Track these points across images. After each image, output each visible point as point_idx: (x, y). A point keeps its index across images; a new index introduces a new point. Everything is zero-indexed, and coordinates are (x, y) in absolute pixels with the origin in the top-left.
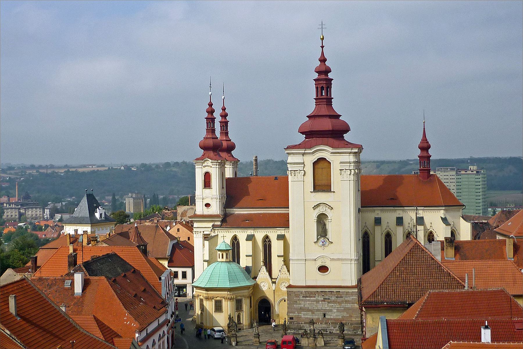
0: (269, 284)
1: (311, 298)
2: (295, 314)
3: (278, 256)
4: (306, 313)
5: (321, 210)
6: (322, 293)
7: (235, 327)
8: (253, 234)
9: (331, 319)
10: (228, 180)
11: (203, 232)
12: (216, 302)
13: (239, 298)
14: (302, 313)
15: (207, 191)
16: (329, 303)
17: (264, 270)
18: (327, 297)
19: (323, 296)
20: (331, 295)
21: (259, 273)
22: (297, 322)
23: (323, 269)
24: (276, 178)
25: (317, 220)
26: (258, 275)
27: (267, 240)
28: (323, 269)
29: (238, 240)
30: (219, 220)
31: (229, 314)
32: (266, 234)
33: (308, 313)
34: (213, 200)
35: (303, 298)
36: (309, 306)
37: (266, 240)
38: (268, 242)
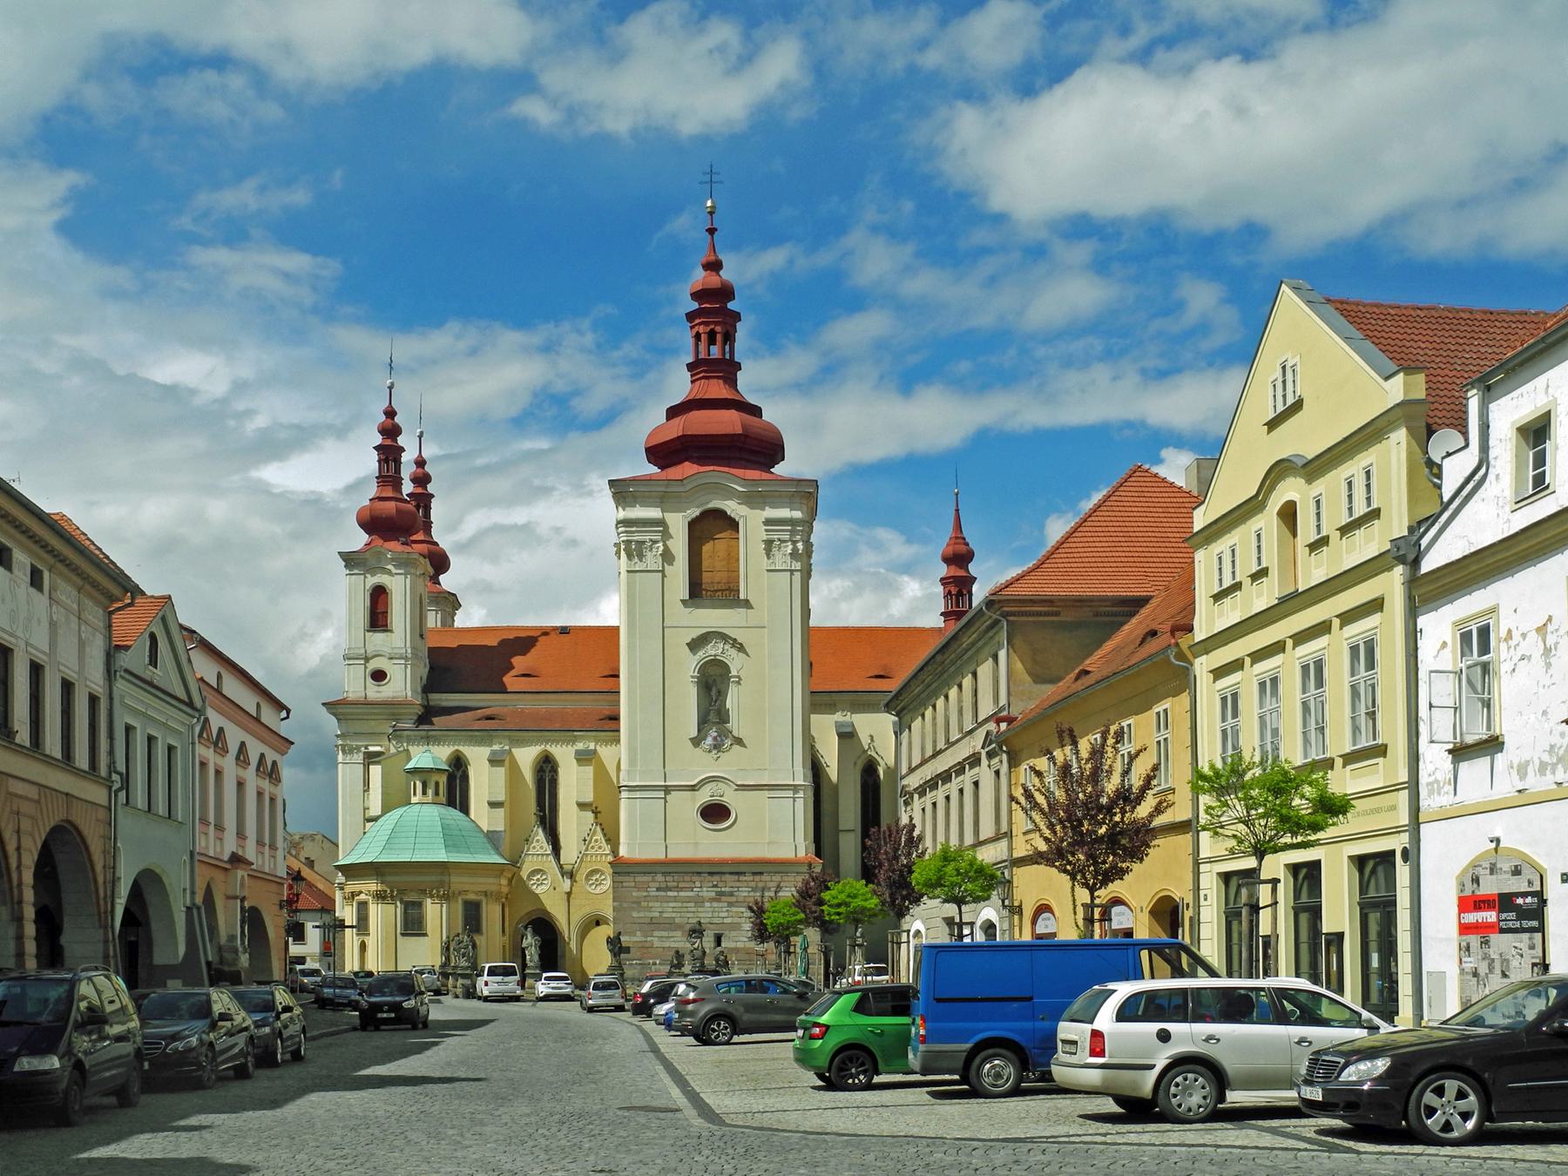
1: (682, 894)
2: (635, 939)
4: (665, 934)
5: (712, 650)
6: (710, 878)
9: (737, 950)
11: (366, 748)
13: (472, 897)
14: (656, 933)
15: (378, 638)
16: (730, 904)
18: (727, 889)
19: (716, 886)
20: (738, 884)
23: (715, 813)
25: (698, 677)
28: (715, 813)
30: (411, 714)
33: (674, 934)
35: (657, 893)
36: (674, 915)
38: (550, 772)
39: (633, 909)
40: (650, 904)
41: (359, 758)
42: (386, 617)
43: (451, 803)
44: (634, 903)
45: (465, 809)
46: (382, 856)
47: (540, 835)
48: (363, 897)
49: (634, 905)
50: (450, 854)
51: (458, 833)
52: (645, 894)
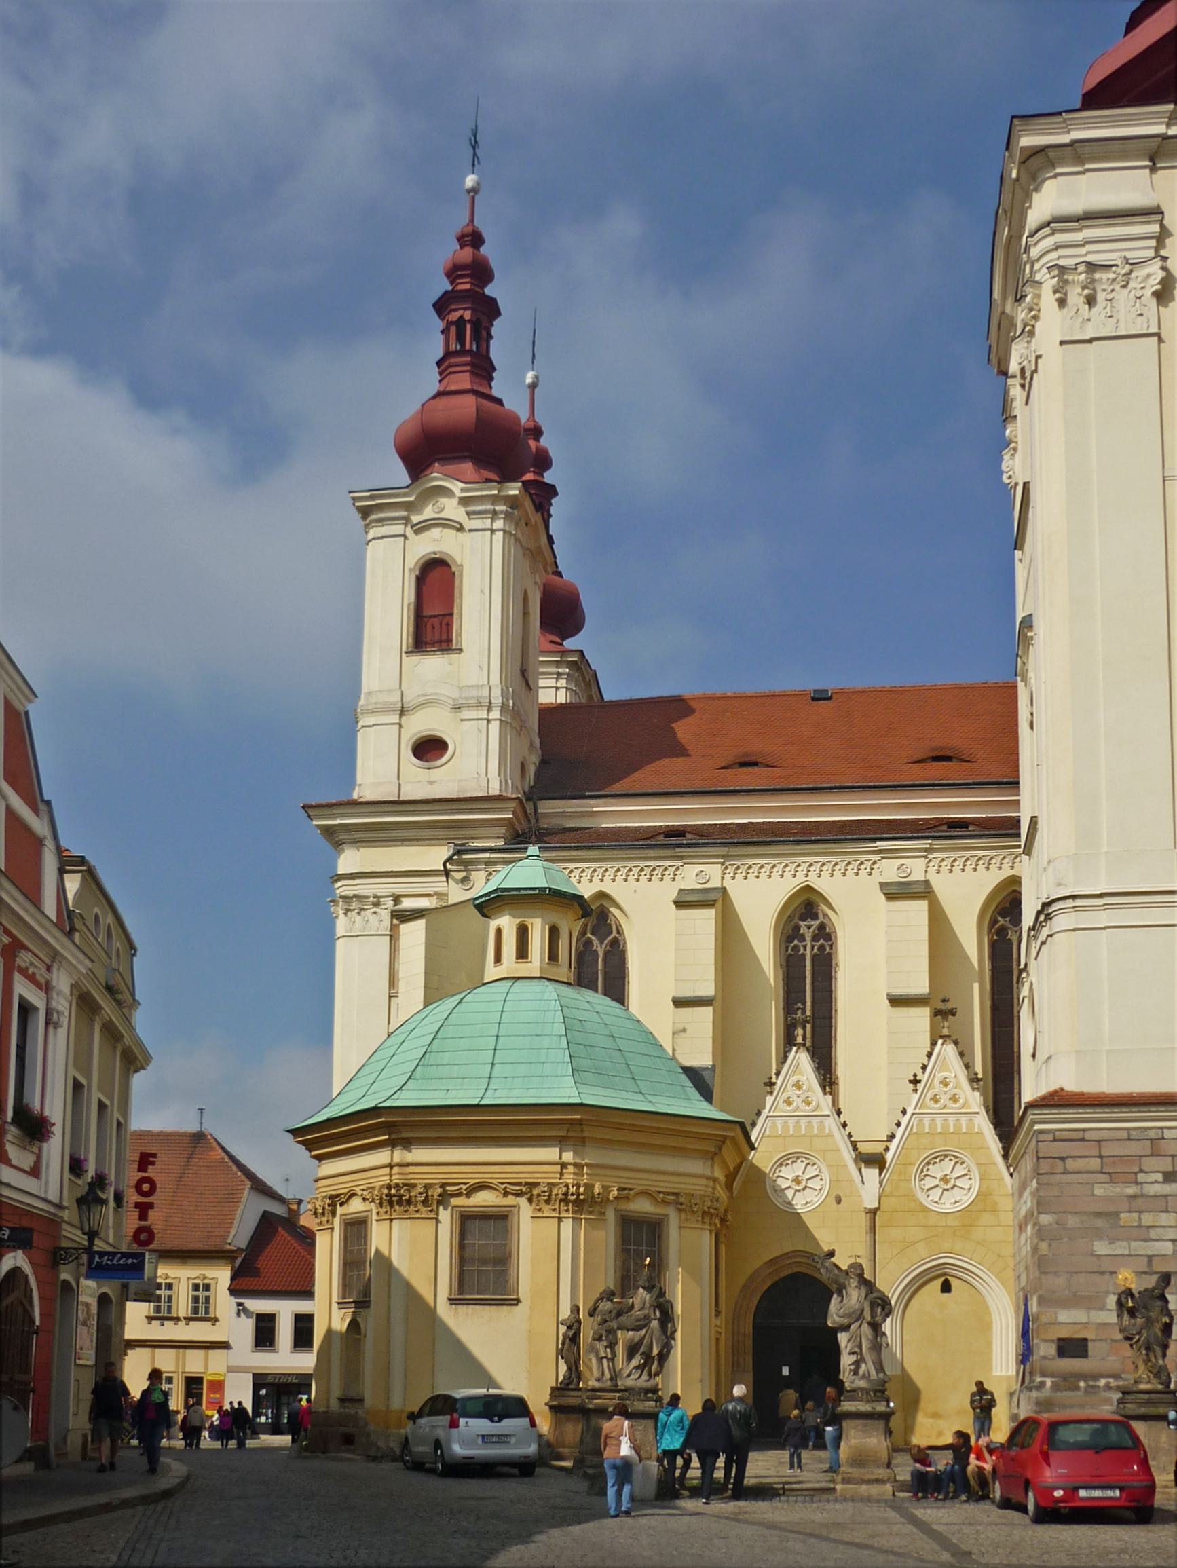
0: (837, 1168)
3: (897, 1001)
7: (655, 1324)
8: (715, 883)
10: (549, 714)
12: (466, 1220)
13: (642, 1206)
15: (432, 664)
17: (803, 1078)
21: (769, 1100)
22: (1116, 1376)
24: (820, 696)
26: (759, 1113)
27: (809, 927)
29: (614, 934)
31: (565, 1313)
32: (800, 880)
34: (466, 714)
37: (797, 928)
38: (815, 938)
39: (1098, 1234)
40: (1147, 1219)
41: (383, 918)
42: (449, 626)
43: (583, 979)
44: (1099, 1214)
45: (616, 989)
46: (403, 1094)
47: (801, 1060)
48: (356, 1206)
49: (1100, 1223)
50: (583, 1089)
51: (609, 1043)
52: (1131, 1190)
